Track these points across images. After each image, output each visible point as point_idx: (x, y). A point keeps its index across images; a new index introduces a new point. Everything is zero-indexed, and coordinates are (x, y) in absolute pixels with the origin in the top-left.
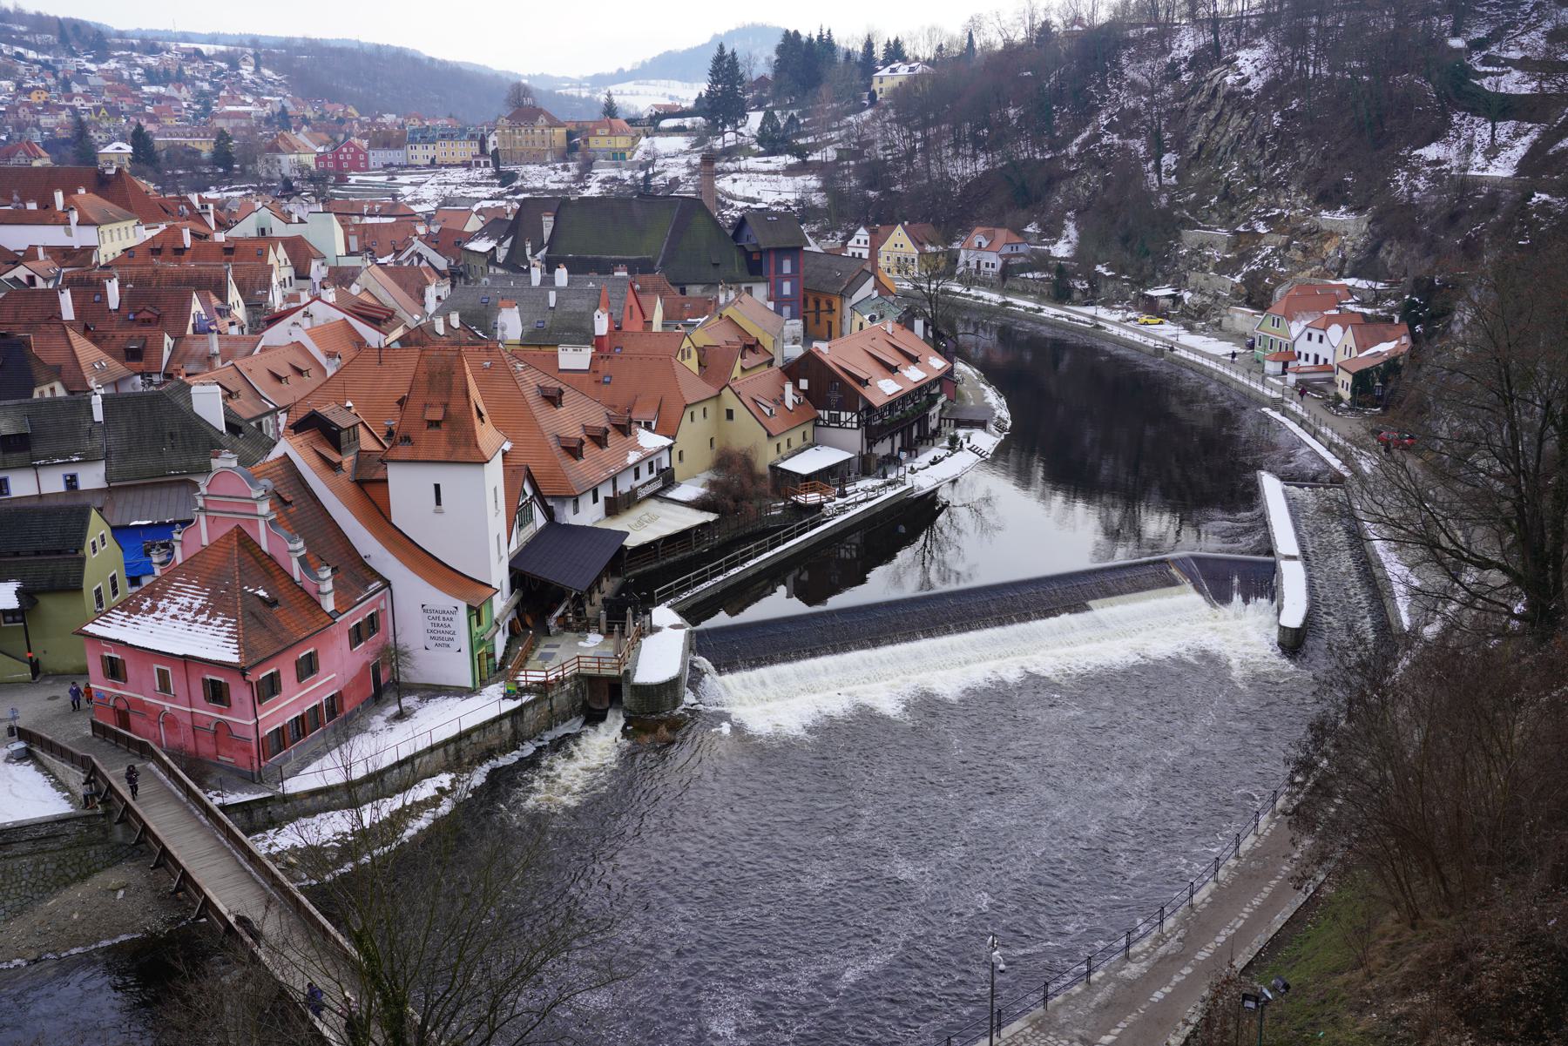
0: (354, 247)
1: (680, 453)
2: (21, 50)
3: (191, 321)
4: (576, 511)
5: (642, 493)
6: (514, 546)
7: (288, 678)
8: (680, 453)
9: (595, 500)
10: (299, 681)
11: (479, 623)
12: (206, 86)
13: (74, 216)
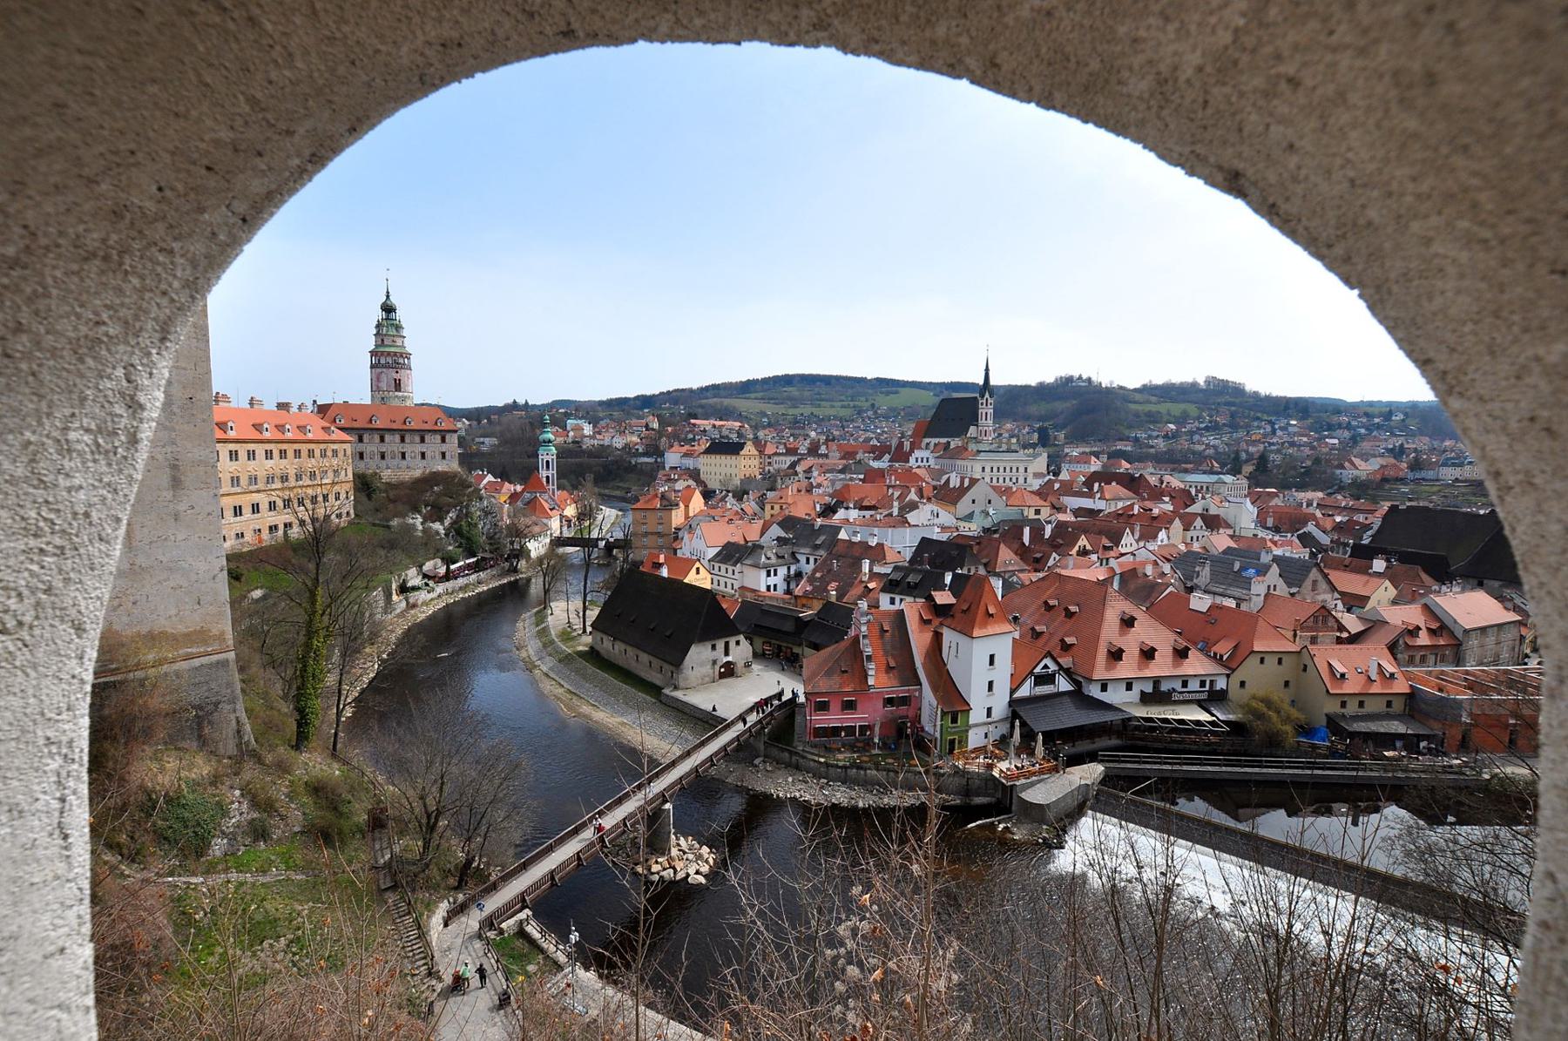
0: (1270, 522)
1: (1243, 684)
2: (1259, 415)
3: (1076, 548)
4: (1104, 688)
5: (1176, 697)
6: (1025, 691)
7: (835, 706)
8: (1243, 684)
9: (1129, 687)
10: (843, 710)
11: (954, 721)
12: (1363, 431)
13: (1098, 495)
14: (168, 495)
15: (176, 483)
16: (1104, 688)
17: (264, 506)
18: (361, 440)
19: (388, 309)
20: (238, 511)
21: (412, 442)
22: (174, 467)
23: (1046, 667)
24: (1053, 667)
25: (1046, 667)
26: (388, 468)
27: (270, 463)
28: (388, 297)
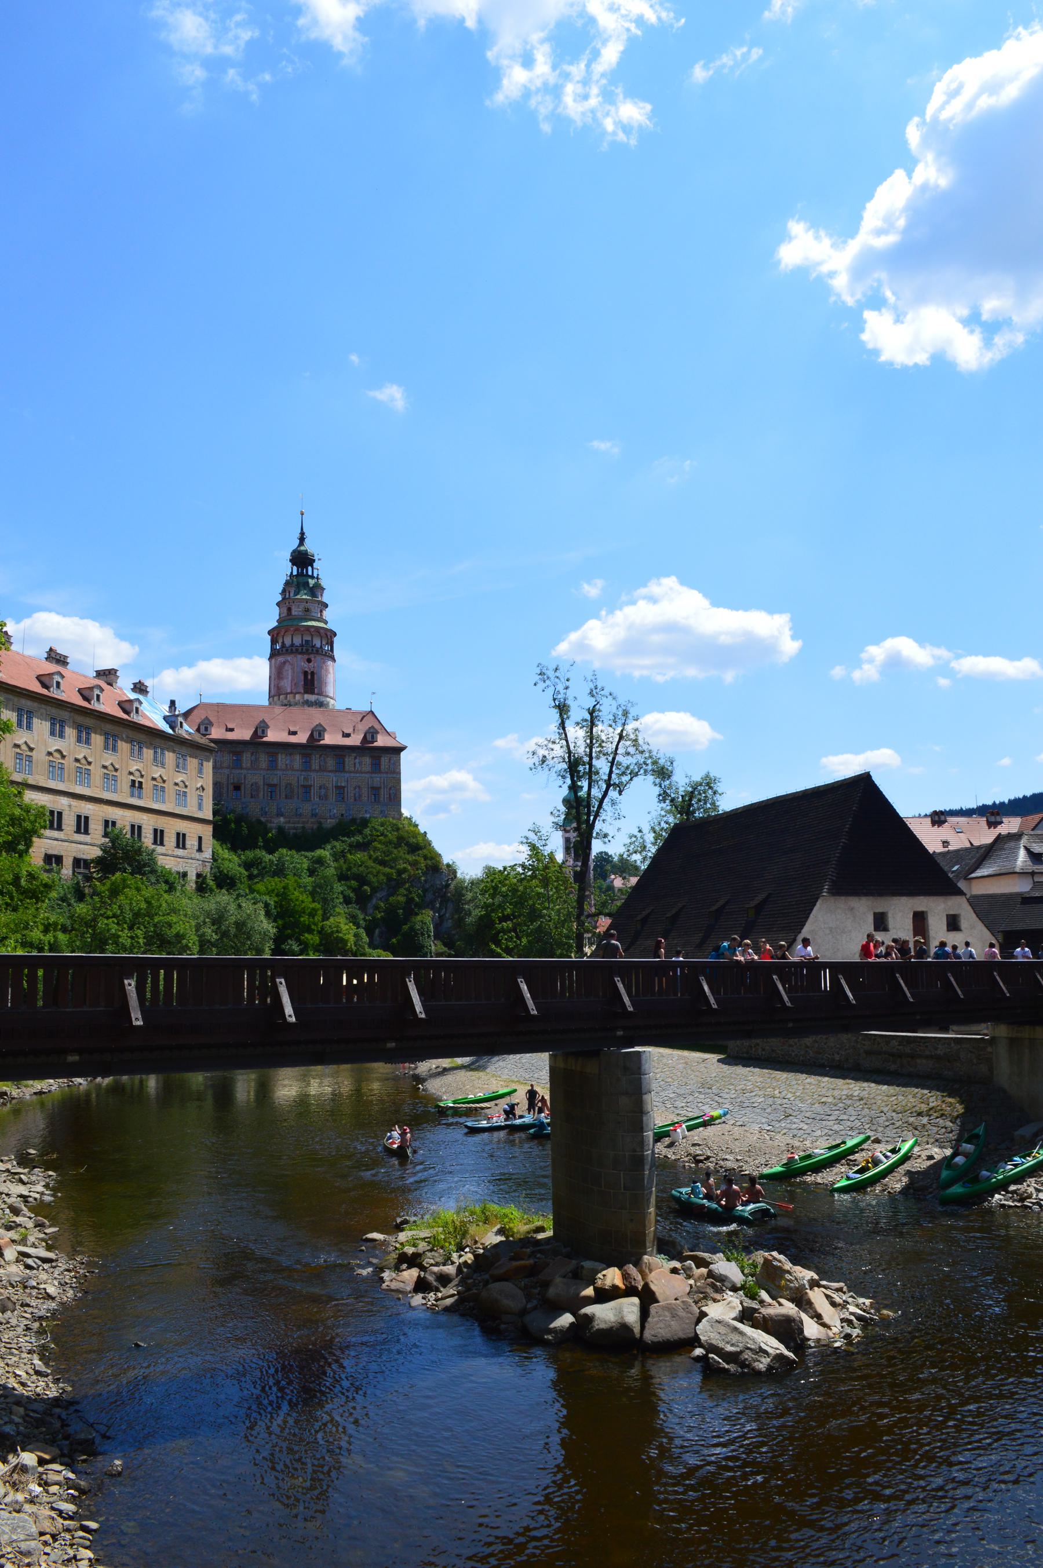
18: (237, 765)
19: (302, 560)
21: (322, 769)
26: (280, 814)
28: (302, 539)
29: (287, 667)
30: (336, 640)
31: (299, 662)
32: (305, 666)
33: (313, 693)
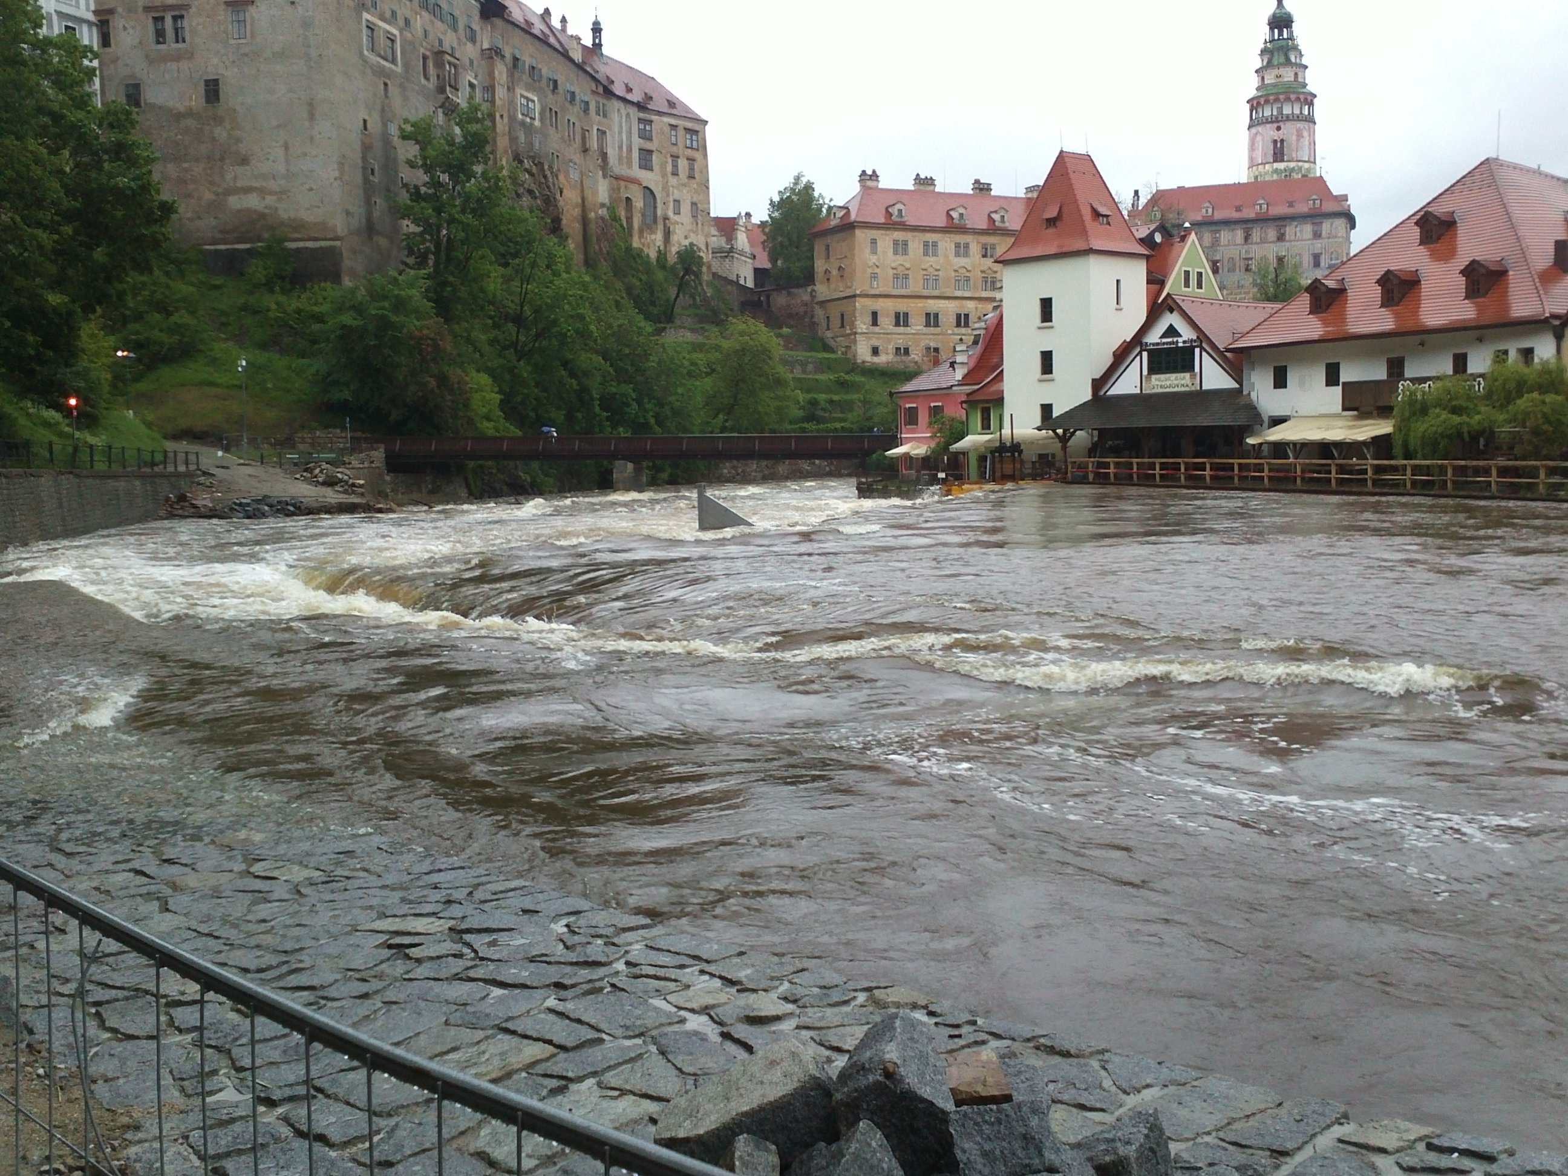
4: (1280, 382)
14: (307, 124)
15: (312, 117)
16: (1280, 382)
17: (948, 320)
19: (1281, 22)
20: (901, 319)
21: (1263, 241)
22: (311, 104)
23: (1171, 331)
24: (1187, 334)
25: (1171, 331)
27: (963, 261)
29: (1259, 138)
30: (1316, 101)
31: (1269, 132)
32: (1277, 135)
33: (1282, 161)
